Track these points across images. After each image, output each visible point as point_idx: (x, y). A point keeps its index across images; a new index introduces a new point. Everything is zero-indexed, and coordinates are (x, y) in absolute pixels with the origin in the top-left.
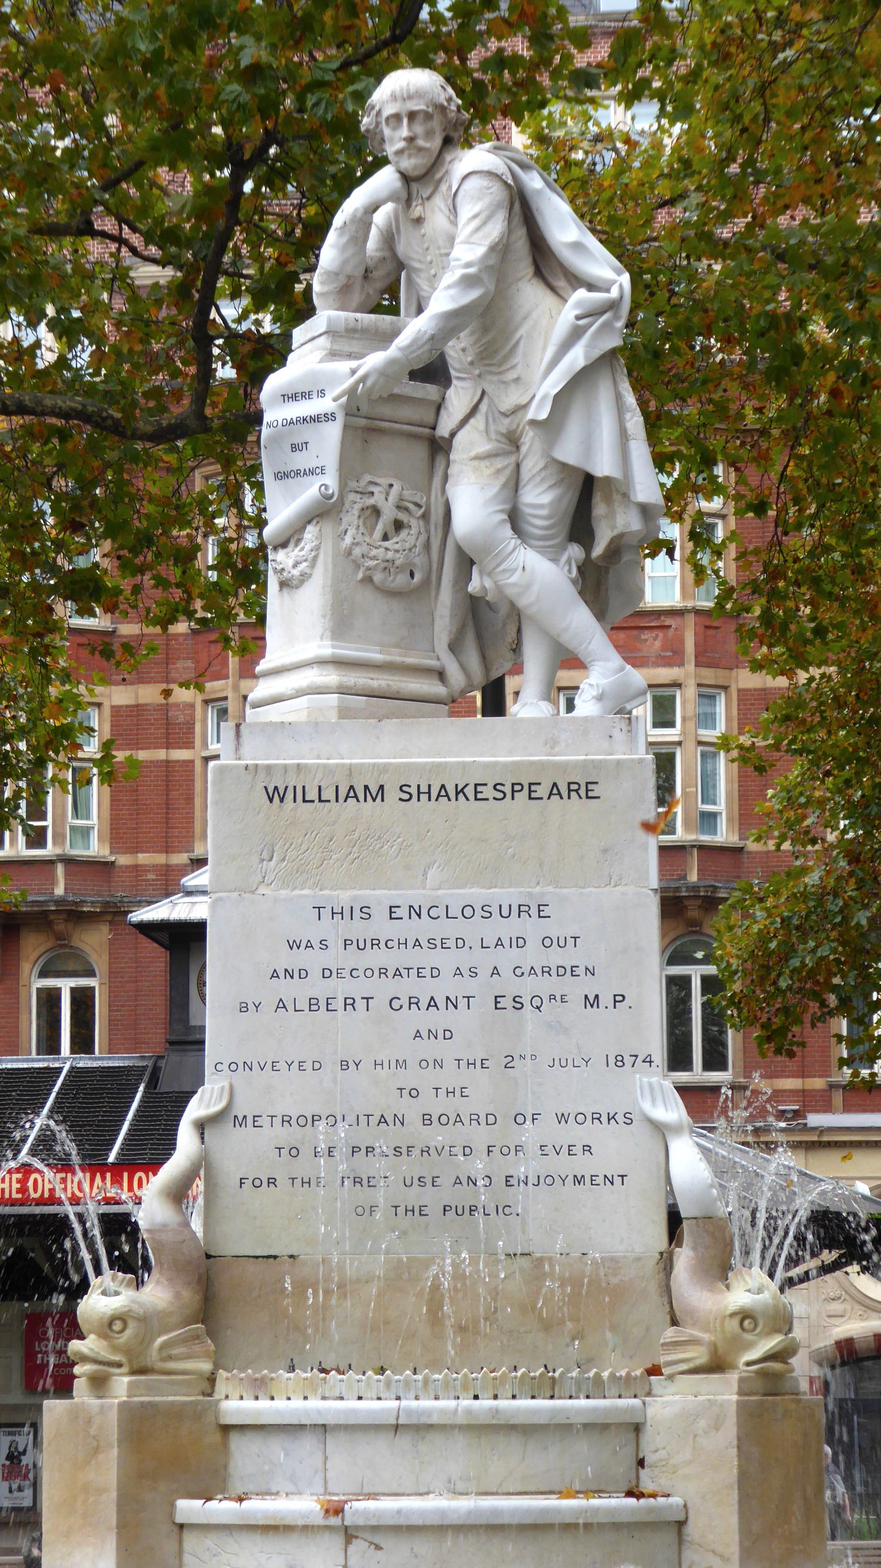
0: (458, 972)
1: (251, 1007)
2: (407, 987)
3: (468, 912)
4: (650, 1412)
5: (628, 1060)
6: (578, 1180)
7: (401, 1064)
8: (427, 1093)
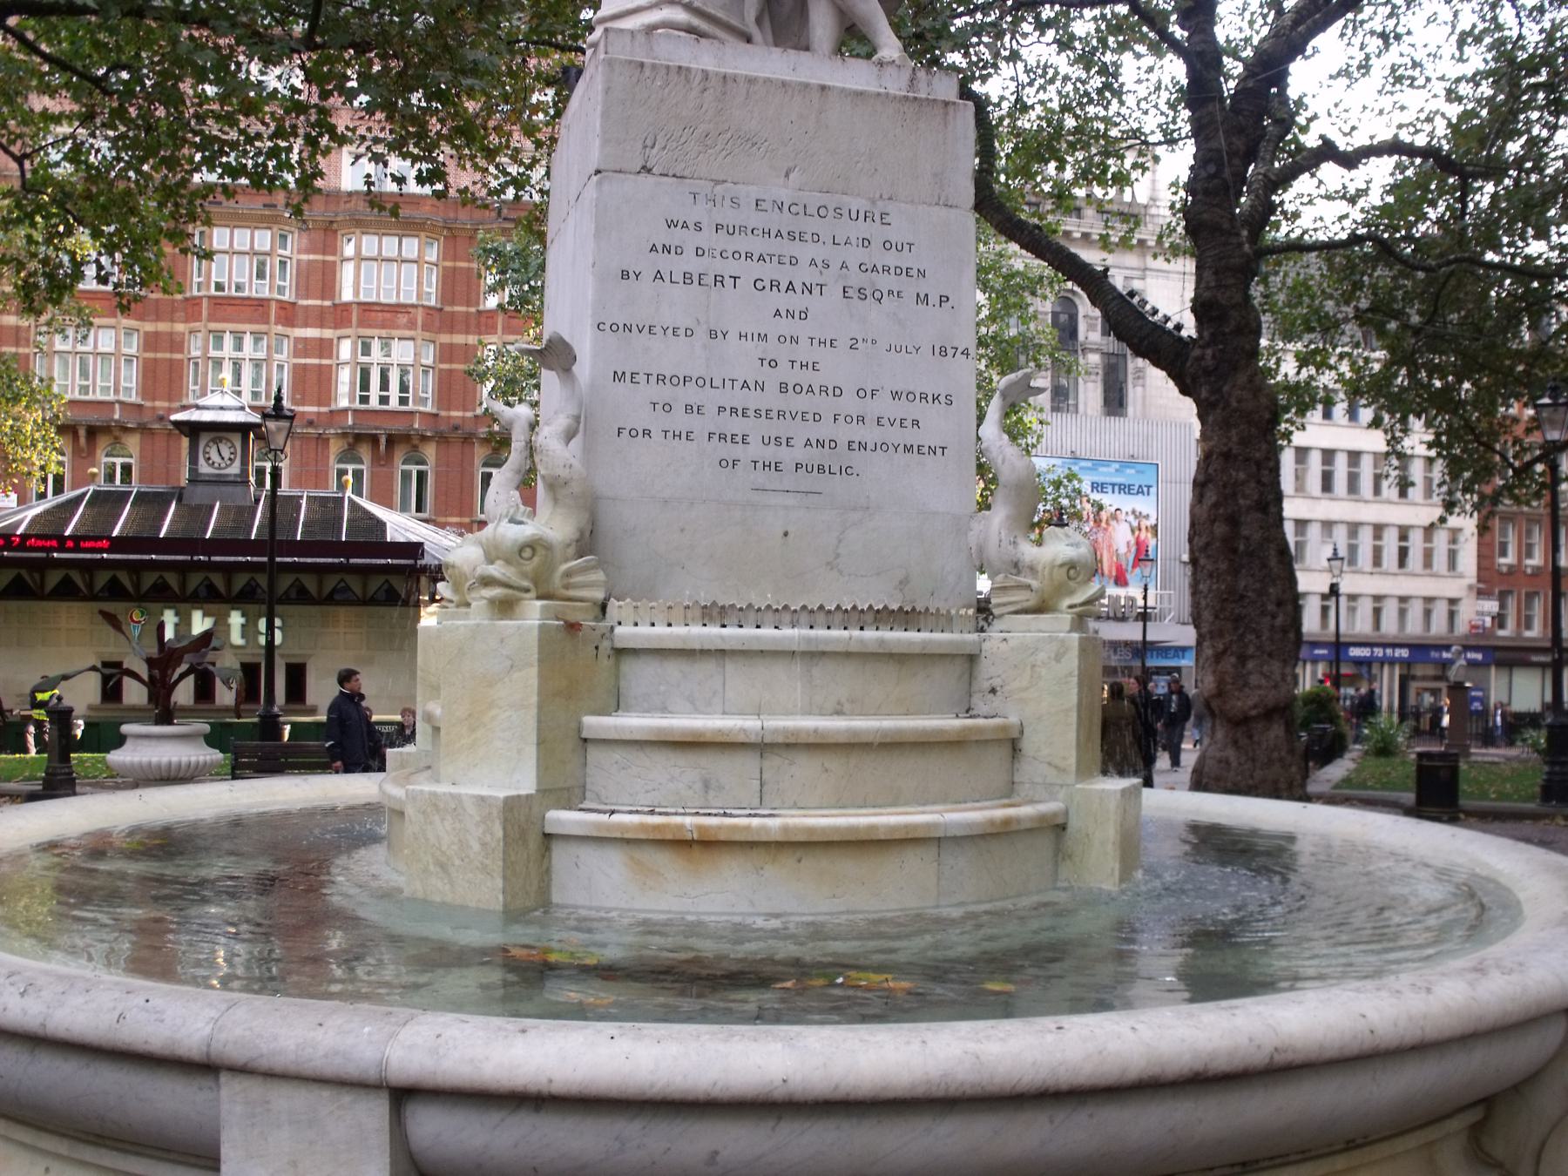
0: (813, 262)
1: (632, 275)
2: (768, 271)
3: (823, 212)
4: (985, 646)
5: (950, 352)
6: (908, 449)
7: (763, 337)
8: (784, 364)
